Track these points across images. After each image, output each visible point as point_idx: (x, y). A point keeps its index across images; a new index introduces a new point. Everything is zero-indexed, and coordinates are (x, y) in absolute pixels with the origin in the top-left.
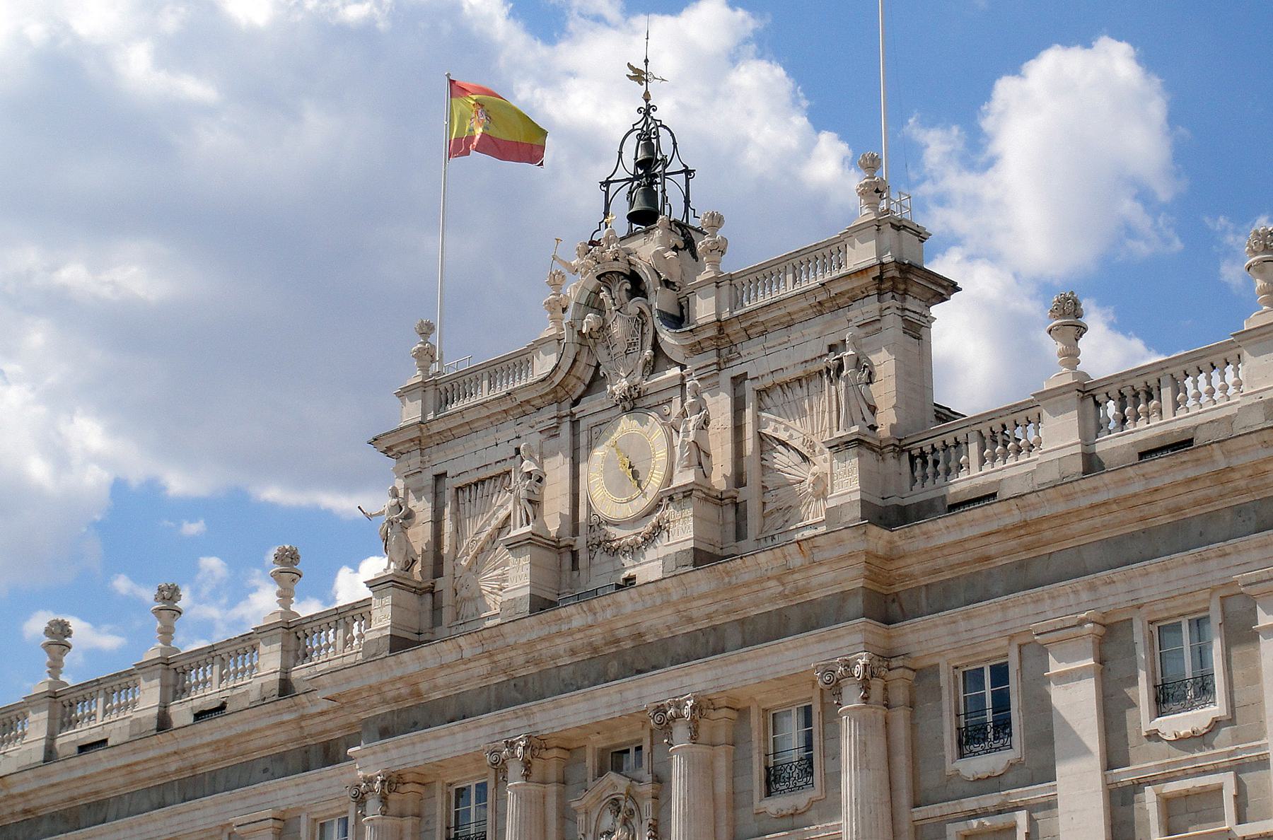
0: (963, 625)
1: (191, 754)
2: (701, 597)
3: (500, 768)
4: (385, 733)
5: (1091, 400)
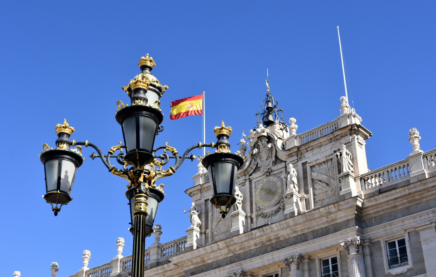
0: (388, 228)
2: (300, 224)
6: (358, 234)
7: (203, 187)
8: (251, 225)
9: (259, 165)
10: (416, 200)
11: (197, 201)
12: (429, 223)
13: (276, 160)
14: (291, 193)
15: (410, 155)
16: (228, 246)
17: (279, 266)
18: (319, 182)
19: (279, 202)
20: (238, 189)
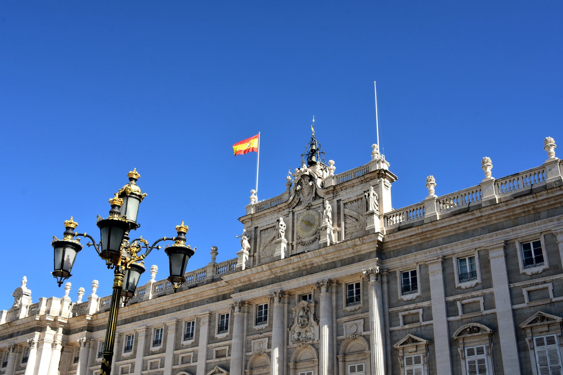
0: (403, 260)
1: (188, 297)
2: (330, 253)
3: (272, 299)
4: (241, 291)
5: (439, 202)
6: (378, 264)
7: (253, 217)
8: (292, 251)
10: (428, 238)
11: (248, 228)
12: (436, 258)
13: (315, 196)
15: (426, 199)
16: (270, 269)
17: (312, 288)
18: (350, 218)
19: (316, 233)
20: (282, 220)
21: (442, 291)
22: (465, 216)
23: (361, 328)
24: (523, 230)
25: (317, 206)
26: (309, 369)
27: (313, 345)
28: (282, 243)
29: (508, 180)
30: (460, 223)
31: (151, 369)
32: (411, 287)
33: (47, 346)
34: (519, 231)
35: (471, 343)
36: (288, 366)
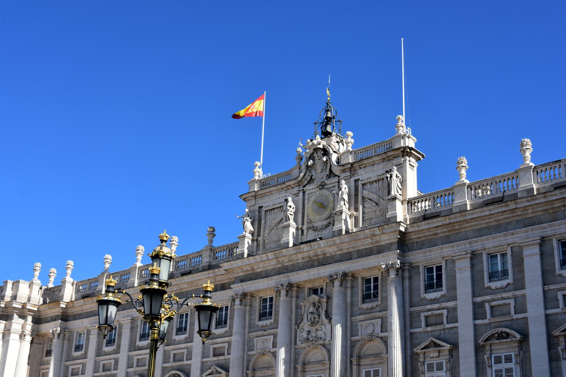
0: (428, 254)
1: (180, 285)
2: (346, 243)
3: (278, 292)
4: (242, 281)
5: (470, 188)
6: (399, 257)
7: (257, 194)
8: (301, 237)
9: (313, 177)
11: (252, 208)
12: (465, 253)
14: (341, 210)
15: (456, 184)
16: (277, 257)
17: (324, 281)
18: (369, 201)
19: (329, 217)
20: (291, 200)
21: (470, 290)
22: (498, 207)
23: (378, 329)
24: (562, 226)
25: (332, 185)
26: (319, 372)
27: (324, 345)
28: (290, 228)
29: (548, 167)
30: (492, 214)
31: (138, 366)
32: (435, 285)
33: (14, 338)
34: (557, 227)
35: (498, 349)
36: (295, 368)
